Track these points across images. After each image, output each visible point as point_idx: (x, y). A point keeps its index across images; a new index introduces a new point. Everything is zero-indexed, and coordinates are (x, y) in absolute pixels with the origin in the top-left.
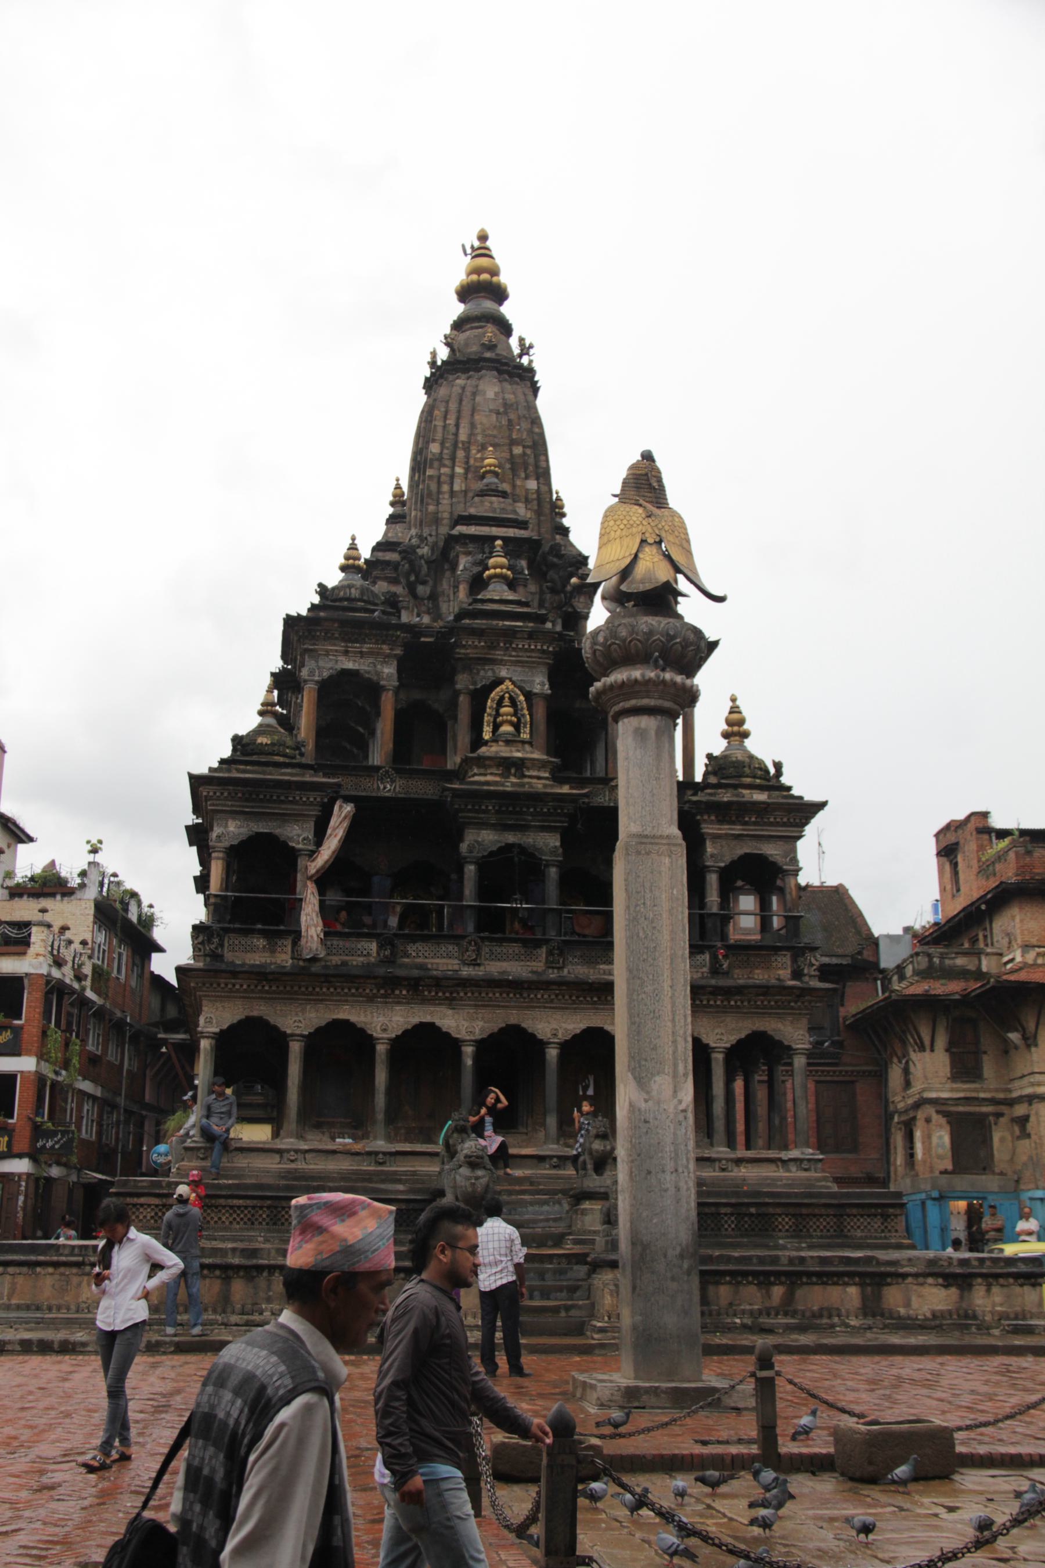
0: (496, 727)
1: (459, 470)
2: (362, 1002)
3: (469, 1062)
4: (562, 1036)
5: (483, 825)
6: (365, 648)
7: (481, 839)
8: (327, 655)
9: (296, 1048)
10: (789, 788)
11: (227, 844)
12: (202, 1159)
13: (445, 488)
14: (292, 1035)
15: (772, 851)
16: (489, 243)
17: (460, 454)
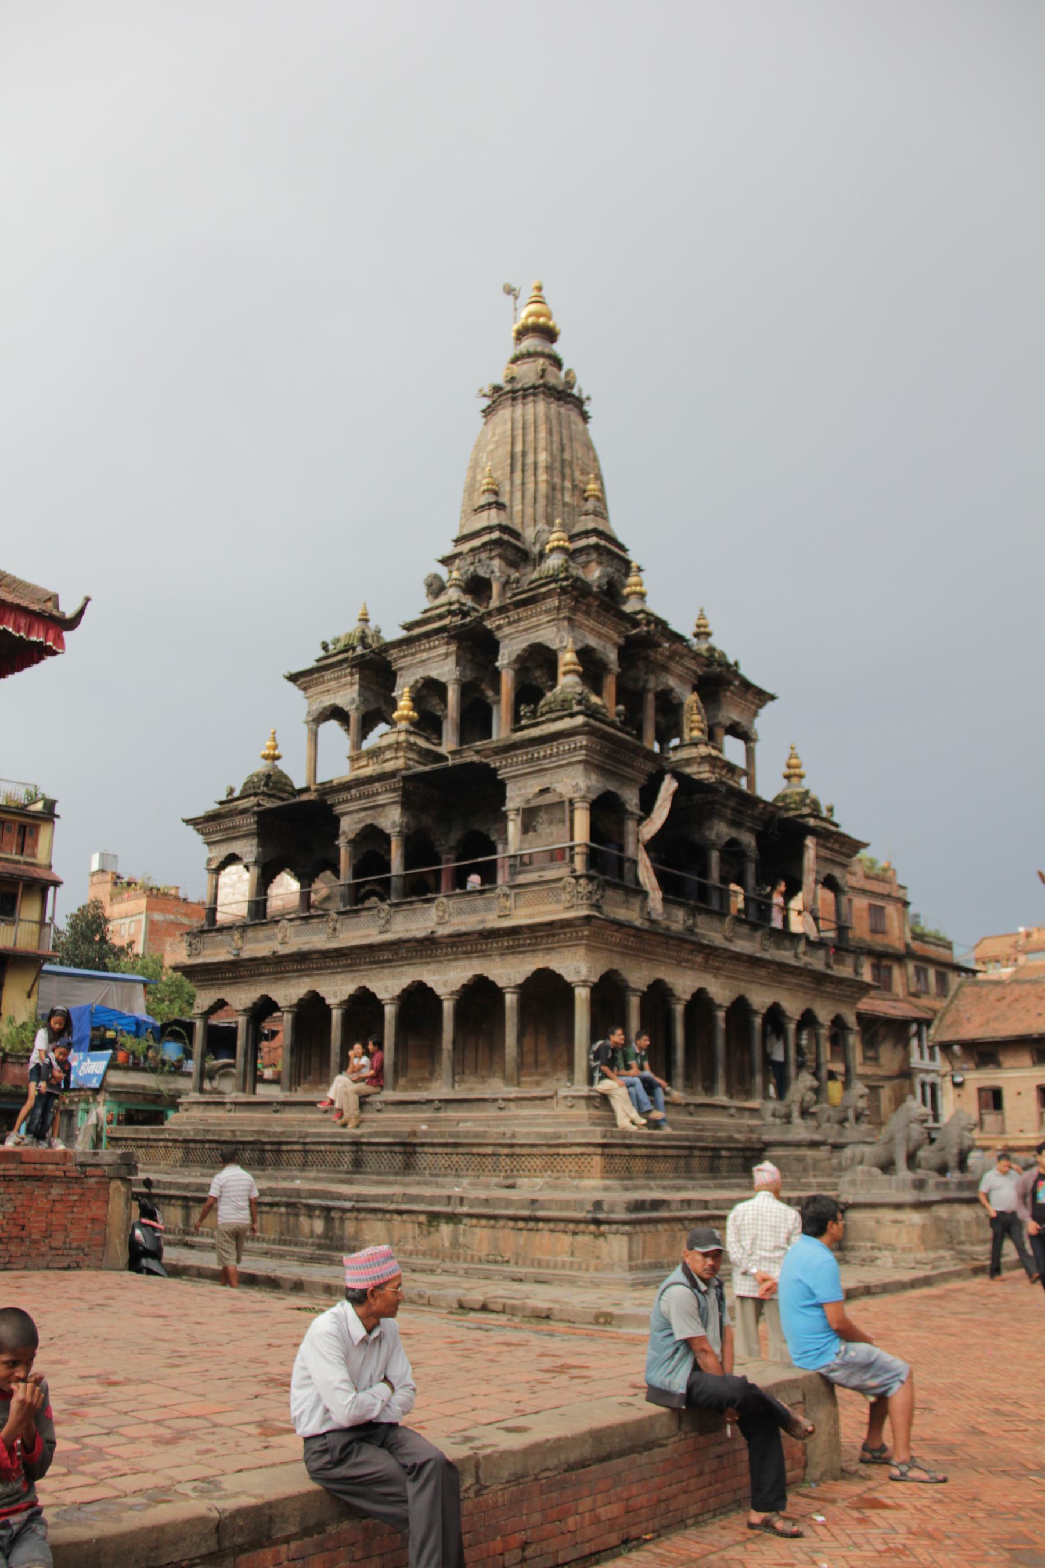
0: (691, 729)
1: (568, 484)
2: (670, 964)
3: (721, 1024)
4: (763, 1011)
5: (722, 817)
6: (604, 630)
7: (720, 831)
8: (580, 627)
9: (634, 1001)
10: (837, 825)
11: (593, 796)
12: (597, 1108)
13: (558, 495)
14: (635, 990)
15: (837, 873)
16: (543, 293)
17: (568, 471)
